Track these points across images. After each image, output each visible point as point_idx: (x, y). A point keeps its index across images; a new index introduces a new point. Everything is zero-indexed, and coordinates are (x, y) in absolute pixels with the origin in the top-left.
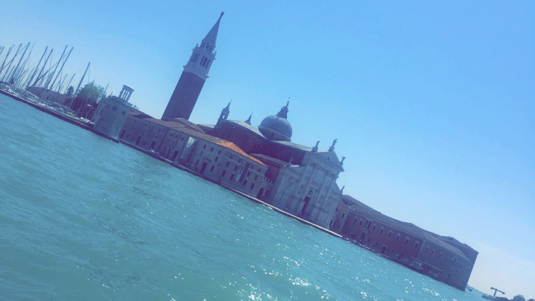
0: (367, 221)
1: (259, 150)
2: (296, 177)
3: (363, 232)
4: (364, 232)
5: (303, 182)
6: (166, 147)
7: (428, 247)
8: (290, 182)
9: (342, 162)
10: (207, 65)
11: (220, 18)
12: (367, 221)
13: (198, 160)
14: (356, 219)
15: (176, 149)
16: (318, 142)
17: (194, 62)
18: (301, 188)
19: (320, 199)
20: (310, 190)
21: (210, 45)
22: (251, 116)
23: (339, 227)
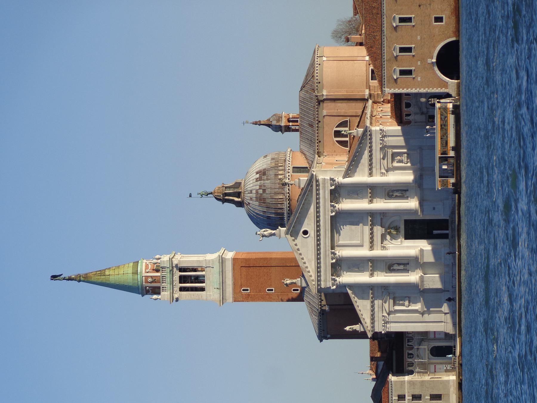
10: (195, 270)
11: (70, 279)
22: (256, 123)
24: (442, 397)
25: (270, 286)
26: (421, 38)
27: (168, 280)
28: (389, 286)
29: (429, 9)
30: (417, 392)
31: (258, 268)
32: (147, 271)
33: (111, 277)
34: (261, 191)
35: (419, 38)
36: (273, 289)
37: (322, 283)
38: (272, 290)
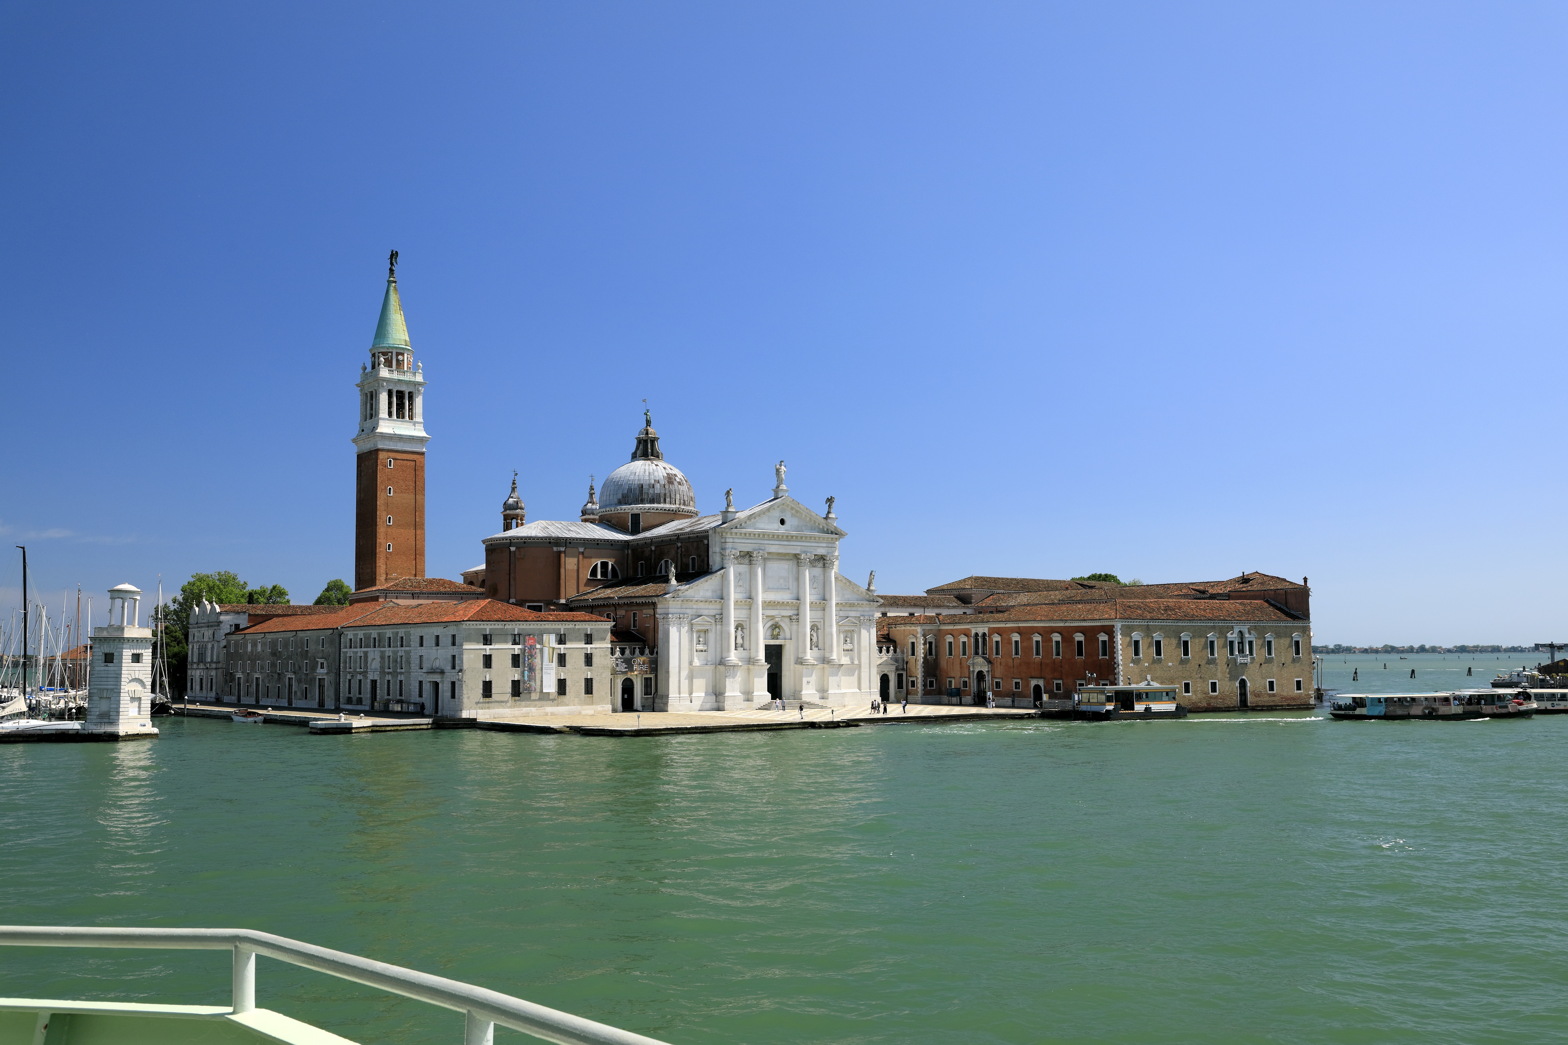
0: (977, 634)
1: (610, 576)
2: (712, 609)
3: (977, 670)
7: (1136, 636)
8: (698, 631)
9: (829, 512)
10: (411, 410)
11: (391, 270)
12: (977, 634)
14: (950, 643)
15: (371, 677)
16: (728, 493)
18: (739, 632)
19: (811, 635)
20: (772, 626)
23: (913, 682)
24: (589, 695)
25: (395, 492)
26: (1170, 667)
27: (402, 378)
28: (722, 625)
29: (1196, 676)
30: (595, 660)
31: (414, 479)
32: (409, 356)
33: (400, 316)
34: (678, 480)
35: (1170, 664)
36: (392, 495)
37: (731, 540)
38: (390, 493)
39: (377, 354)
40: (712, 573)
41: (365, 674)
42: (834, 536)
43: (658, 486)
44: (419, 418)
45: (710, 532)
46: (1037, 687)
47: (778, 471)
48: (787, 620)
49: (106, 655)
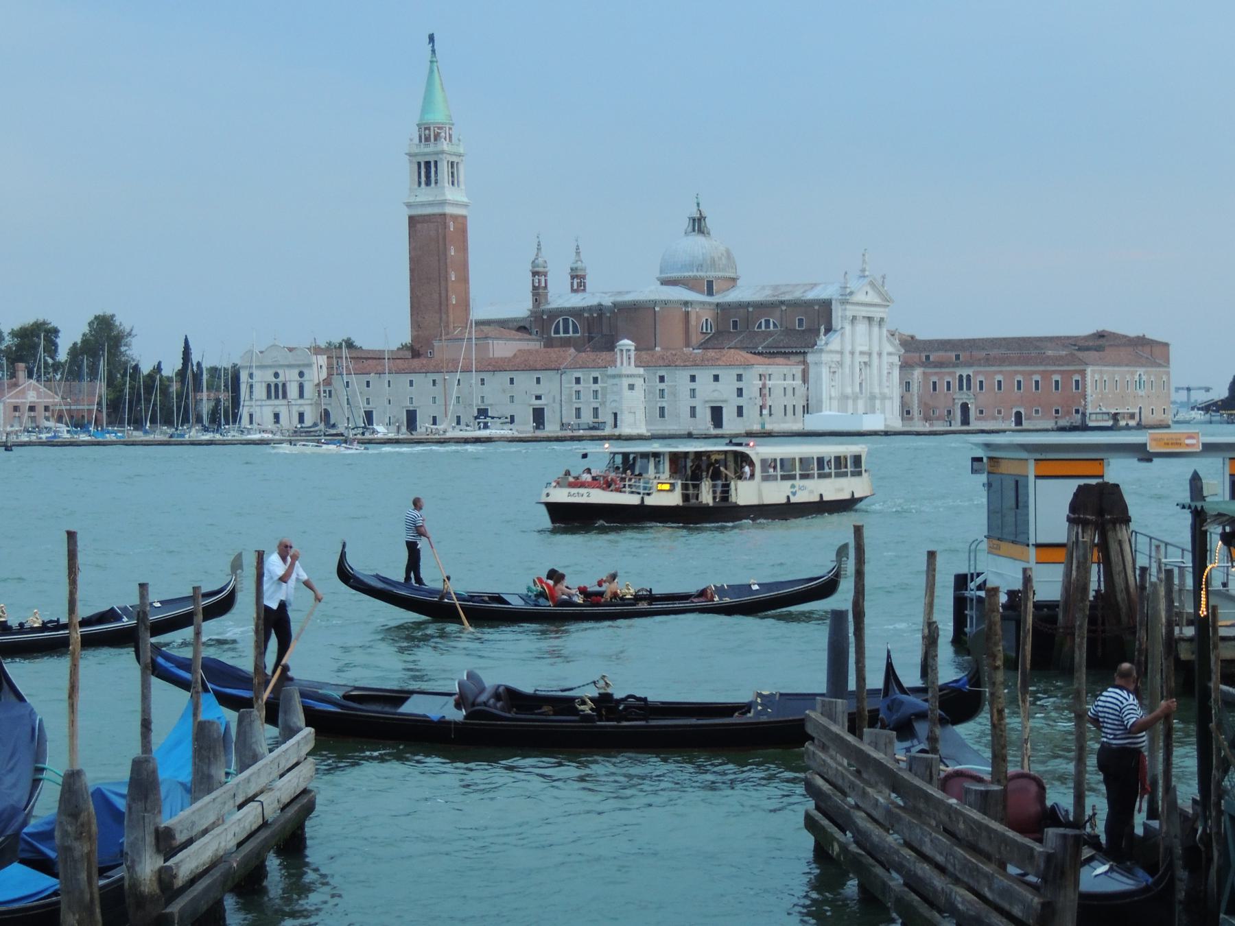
0: (961, 376)
1: (709, 331)
2: (837, 357)
3: (960, 402)
4: (965, 401)
5: (848, 359)
6: (578, 410)
7: (1097, 377)
11: (433, 51)
12: (961, 376)
13: (693, 409)
14: (934, 383)
16: (846, 273)
17: (428, 183)
21: (447, 126)
22: (578, 247)
23: (908, 412)
39: (432, 128)
40: (836, 331)
41: (603, 403)
42: (888, 304)
43: (723, 258)
44: (462, 186)
45: (833, 302)
46: (1018, 415)
47: (864, 255)
48: (863, 366)
49: (629, 385)
